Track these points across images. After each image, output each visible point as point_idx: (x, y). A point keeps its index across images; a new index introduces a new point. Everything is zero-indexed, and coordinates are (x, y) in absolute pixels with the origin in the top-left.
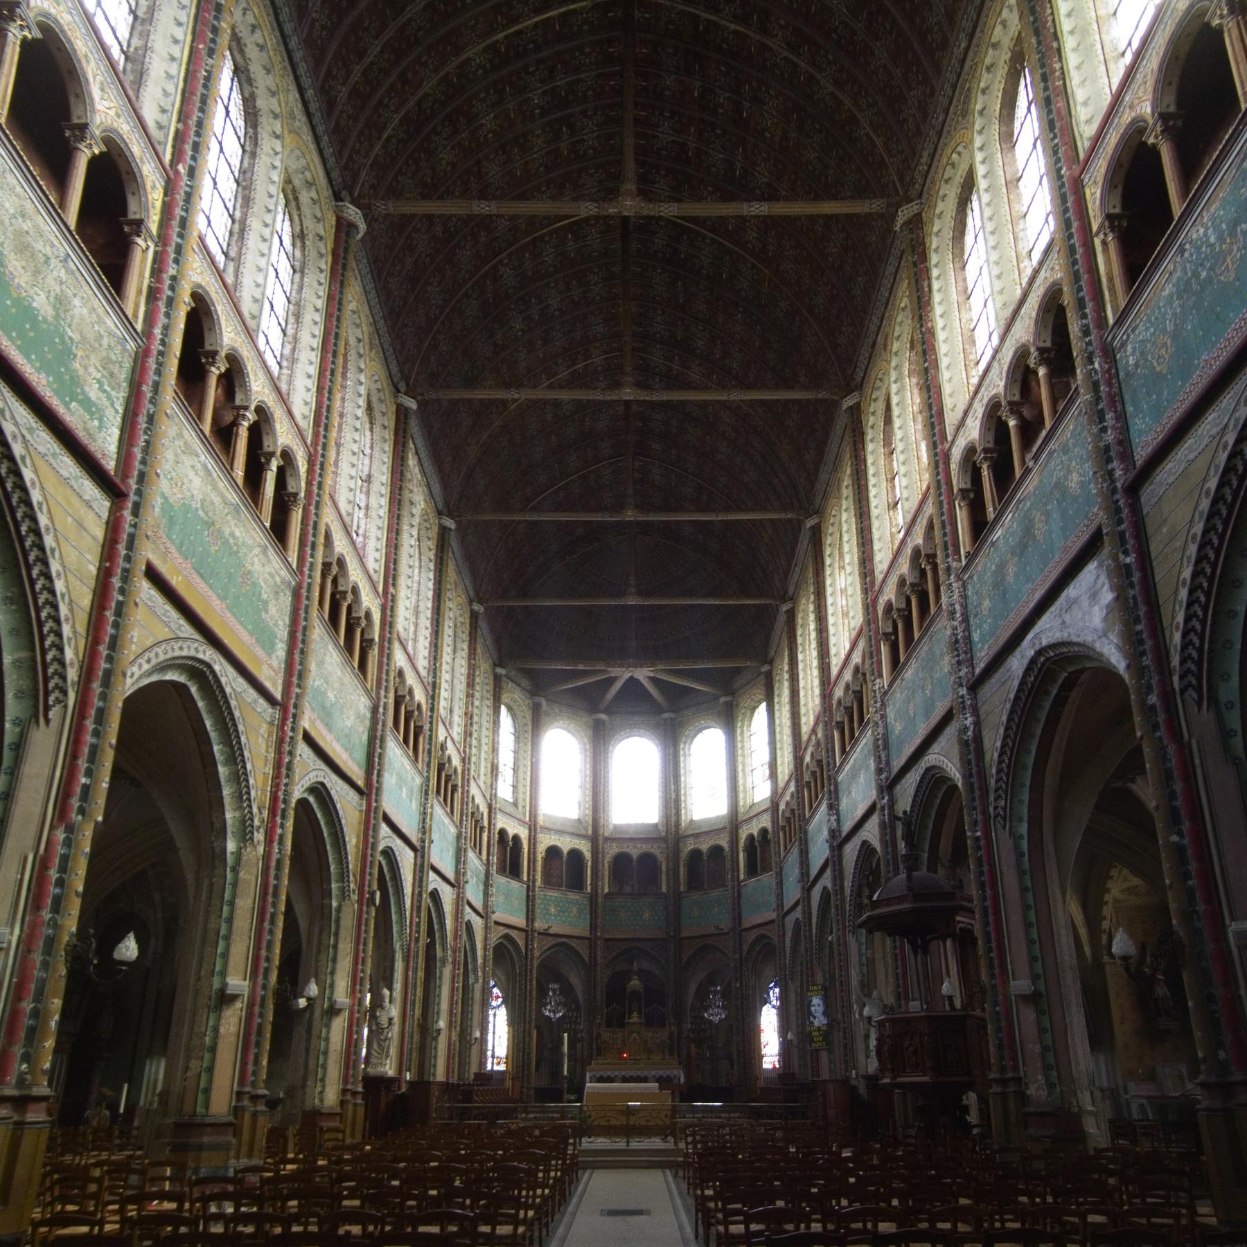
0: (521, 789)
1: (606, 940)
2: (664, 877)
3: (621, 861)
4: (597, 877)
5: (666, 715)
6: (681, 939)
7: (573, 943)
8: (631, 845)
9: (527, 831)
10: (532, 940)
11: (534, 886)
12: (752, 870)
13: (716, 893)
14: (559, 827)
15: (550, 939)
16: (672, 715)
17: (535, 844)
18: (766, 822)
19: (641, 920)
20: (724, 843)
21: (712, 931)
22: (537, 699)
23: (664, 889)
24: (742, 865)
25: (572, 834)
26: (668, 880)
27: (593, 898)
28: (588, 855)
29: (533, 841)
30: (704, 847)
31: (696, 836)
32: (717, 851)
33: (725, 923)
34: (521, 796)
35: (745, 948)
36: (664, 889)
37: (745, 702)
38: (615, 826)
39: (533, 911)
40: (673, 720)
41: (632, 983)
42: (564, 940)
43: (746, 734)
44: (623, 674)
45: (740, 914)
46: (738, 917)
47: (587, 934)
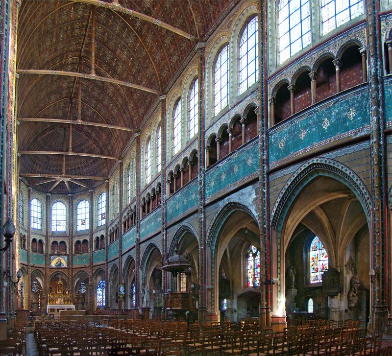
2: (68, 249)
3: (55, 243)
5: (70, 195)
12: (97, 247)
13: (84, 254)
18: (103, 233)
20: (88, 238)
24: (93, 246)
30: (81, 240)
32: (85, 241)
34: (25, 222)
40: (72, 197)
44: (59, 179)
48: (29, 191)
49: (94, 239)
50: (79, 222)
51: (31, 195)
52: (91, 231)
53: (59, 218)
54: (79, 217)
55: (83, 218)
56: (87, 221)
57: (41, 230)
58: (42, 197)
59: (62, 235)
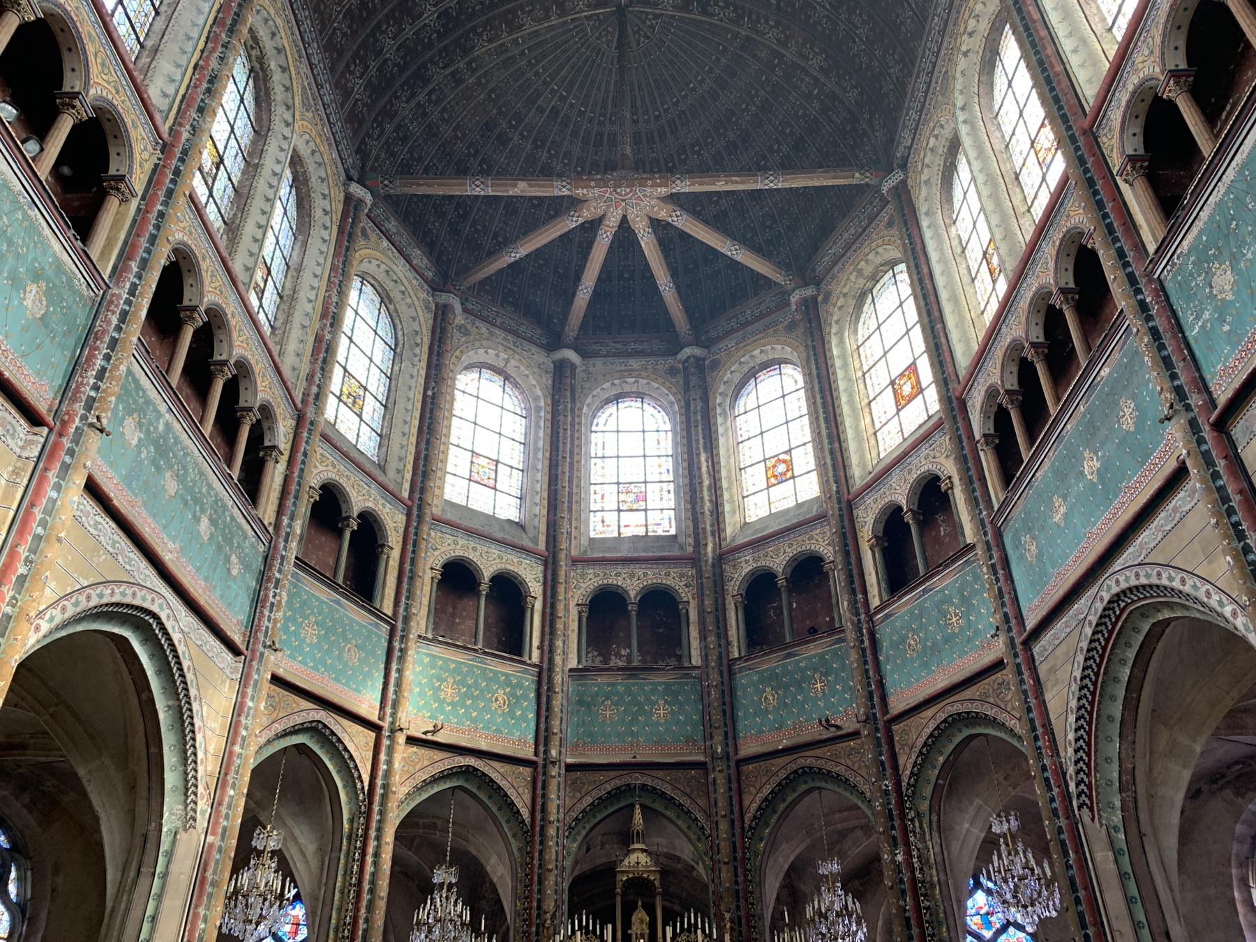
0: (396, 438)
1: (570, 768)
2: (694, 633)
4: (553, 632)
6: (739, 763)
7: (494, 771)
8: (624, 571)
9: (401, 518)
10: (391, 750)
13: (813, 651)
15: (439, 755)
16: (697, 351)
19: (647, 722)
20: (823, 544)
21: (814, 732)
22: (444, 298)
23: (696, 660)
26: (703, 637)
27: (544, 675)
28: (535, 588)
29: (412, 541)
30: (778, 561)
31: (758, 544)
32: (808, 569)
33: (848, 714)
35: (907, 762)
36: (696, 660)
37: (846, 282)
39: (399, 684)
40: (699, 361)
41: (633, 858)
42: (471, 761)
43: (850, 344)
45: (881, 684)
46: (877, 691)
47: (528, 753)
48: (441, 316)
49: (866, 533)
50: (754, 478)
51: (456, 337)
52: (842, 499)
53: (631, 471)
54: (750, 453)
55: (776, 444)
56: (805, 460)
57: (520, 526)
58: (532, 365)
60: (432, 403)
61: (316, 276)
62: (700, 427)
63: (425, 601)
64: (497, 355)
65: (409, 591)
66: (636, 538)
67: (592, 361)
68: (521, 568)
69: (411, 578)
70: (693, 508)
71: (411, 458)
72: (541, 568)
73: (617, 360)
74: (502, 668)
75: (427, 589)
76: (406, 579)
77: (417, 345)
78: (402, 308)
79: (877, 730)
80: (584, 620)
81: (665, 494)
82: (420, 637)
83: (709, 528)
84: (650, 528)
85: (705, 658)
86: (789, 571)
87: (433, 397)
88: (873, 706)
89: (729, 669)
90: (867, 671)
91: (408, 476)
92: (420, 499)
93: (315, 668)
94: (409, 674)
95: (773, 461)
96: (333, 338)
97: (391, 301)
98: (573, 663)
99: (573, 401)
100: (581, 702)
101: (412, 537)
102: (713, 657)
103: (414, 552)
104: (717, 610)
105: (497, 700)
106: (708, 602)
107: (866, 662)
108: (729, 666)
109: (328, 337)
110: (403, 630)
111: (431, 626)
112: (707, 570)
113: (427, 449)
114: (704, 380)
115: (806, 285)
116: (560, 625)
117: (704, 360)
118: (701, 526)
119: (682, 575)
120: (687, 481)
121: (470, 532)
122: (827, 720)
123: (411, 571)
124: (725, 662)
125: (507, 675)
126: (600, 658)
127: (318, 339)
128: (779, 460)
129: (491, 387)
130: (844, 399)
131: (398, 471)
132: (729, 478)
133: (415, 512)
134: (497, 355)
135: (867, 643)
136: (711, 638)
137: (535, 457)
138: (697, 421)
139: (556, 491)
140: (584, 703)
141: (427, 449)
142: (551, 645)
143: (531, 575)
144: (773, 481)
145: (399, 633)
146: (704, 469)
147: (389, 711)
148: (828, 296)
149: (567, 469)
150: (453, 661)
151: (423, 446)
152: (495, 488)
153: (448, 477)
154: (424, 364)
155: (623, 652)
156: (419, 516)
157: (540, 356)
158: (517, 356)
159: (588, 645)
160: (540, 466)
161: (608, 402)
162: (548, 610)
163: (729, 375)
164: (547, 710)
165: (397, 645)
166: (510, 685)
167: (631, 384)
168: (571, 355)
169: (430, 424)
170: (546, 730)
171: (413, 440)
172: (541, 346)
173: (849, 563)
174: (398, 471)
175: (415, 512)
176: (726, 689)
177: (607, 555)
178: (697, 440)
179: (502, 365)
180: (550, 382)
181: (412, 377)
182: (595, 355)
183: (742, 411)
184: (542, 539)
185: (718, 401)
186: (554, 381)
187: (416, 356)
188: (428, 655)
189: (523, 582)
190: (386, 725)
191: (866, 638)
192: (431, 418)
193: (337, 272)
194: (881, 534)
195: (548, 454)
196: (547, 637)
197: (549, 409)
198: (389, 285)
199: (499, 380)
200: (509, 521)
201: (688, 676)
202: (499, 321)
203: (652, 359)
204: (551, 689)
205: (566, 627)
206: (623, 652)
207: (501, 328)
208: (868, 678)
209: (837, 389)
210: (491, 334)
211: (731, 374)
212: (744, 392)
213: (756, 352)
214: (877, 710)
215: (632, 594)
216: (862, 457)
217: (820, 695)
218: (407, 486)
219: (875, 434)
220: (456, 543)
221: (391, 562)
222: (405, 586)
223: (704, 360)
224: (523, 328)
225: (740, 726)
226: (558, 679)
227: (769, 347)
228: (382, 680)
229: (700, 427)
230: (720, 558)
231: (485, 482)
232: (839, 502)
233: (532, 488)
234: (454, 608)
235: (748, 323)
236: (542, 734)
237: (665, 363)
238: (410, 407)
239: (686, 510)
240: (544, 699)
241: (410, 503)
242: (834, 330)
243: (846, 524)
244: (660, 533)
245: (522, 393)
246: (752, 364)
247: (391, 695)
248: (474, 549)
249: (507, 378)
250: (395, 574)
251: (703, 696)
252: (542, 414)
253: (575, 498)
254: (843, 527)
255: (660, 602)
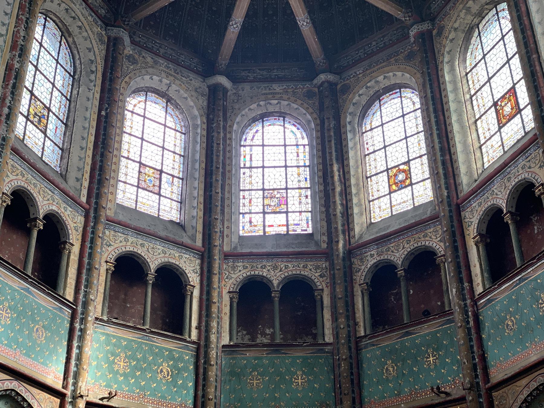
2: (327, 315)
8: (269, 264)
9: (80, 219)
11: (85, 312)
13: (426, 330)
14: (142, 225)
16: (331, 77)
17: (92, 241)
20: (435, 240)
22: (115, 32)
23: (329, 338)
25: (166, 240)
26: (335, 318)
27: (201, 350)
28: (194, 278)
29: (89, 238)
30: (398, 254)
31: (383, 240)
32: (423, 262)
36: (329, 338)
38: (241, 238)
39: (79, 358)
40: (332, 85)
43: (459, 71)
45: (483, 358)
46: (480, 363)
48: (113, 47)
49: (472, 231)
53: (275, 179)
54: (376, 163)
55: (397, 156)
56: (421, 170)
57: (181, 226)
58: (189, 90)
59: (292, 247)
60: (106, 122)
61: (6, 14)
62: (333, 142)
63: (101, 289)
64: (161, 81)
65: (87, 280)
66: (278, 236)
67: (241, 86)
68: (182, 261)
69: (89, 270)
70: (327, 211)
71: (88, 168)
72: (198, 261)
73: (263, 85)
74: (166, 345)
75: (103, 278)
76: (85, 271)
77: (92, 72)
78: (79, 40)
79: (480, 396)
80: (235, 305)
81: (304, 200)
82: (97, 319)
83: (340, 228)
84: (291, 228)
85: (336, 336)
86: (407, 263)
87: (107, 117)
88: (477, 376)
89: (356, 345)
90: (472, 347)
91: (86, 184)
92: (96, 203)
93: (9, 345)
94: (89, 350)
95: (395, 170)
96: (21, 66)
97: (70, 35)
98: (226, 340)
99: (225, 120)
100: (232, 373)
101: (90, 235)
102: (343, 334)
103: (91, 248)
104: (346, 296)
105: (162, 371)
106: (339, 289)
107: (471, 340)
108: (357, 343)
109: (17, 65)
110: (83, 314)
111: (106, 310)
112: (339, 263)
113: (101, 161)
114: (336, 102)
115: (423, 21)
116: (214, 309)
117: (336, 84)
118: (334, 226)
119: (317, 267)
120: (322, 188)
121: (139, 231)
122: (438, 388)
123: (89, 264)
124: (353, 339)
125: (171, 351)
126: (248, 337)
127: (9, 68)
128: (400, 171)
129: (156, 109)
130: (454, 118)
131: (78, 180)
132: (357, 185)
133: (92, 215)
134: (161, 81)
135: (472, 323)
136: (342, 320)
137: (193, 168)
138: (330, 136)
139: (211, 196)
140: (235, 374)
141: (101, 161)
142: (208, 326)
143: (190, 267)
144: (394, 187)
145: (79, 316)
146: (336, 178)
147: (71, 381)
148: (441, 30)
149: (220, 178)
150: (125, 339)
151: (98, 158)
152: (159, 194)
153: (121, 185)
154: (98, 89)
155: (268, 331)
156: (95, 217)
157: (197, 82)
158: (177, 82)
159: (238, 326)
160: (197, 175)
161: (254, 120)
162: (204, 297)
163: (357, 98)
164: (205, 379)
165: (77, 326)
166: (173, 359)
167: (274, 105)
168: (223, 80)
169: (104, 140)
170: (203, 396)
171: (90, 153)
172: (197, 73)
173: (457, 257)
174: (78, 180)
175: (92, 215)
176: (354, 362)
177: (255, 251)
178: (331, 153)
179: (164, 89)
180: (205, 103)
181: (88, 99)
182: (244, 80)
183: (368, 128)
184: (199, 237)
185: (348, 120)
186: (209, 103)
187: (91, 81)
188: (103, 334)
189: (183, 273)
190: (68, 392)
191: (471, 320)
192: (104, 135)
193: (24, 10)
194: (484, 232)
195: (203, 165)
196: (204, 319)
197: (205, 126)
198: (68, 21)
199: (162, 102)
200: (171, 222)
201: (322, 351)
202: (162, 51)
203: (292, 85)
204: (207, 361)
205: (219, 311)
206: (268, 331)
207: (164, 57)
208: (473, 352)
209: (448, 110)
210: (156, 62)
211: (359, 97)
212: (370, 112)
213: (381, 78)
214: (480, 380)
215: (275, 283)
216: (469, 167)
217: (432, 367)
218: (85, 192)
219: (480, 147)
220: (126, 240)
221: (72, 257)
222: (84, 277)
223: (336, 84)
224: (182, 58)
225: (365, 393)
226: (213, 353)
227: (391, 74)
228: (65, 355)
229: (333, 142)
230: (350, 253)
231: (151, 189)
232: (450, 205)
233: (191, 193)
234: (126, 295)
235: (373, 54)
236: (200, 400)
237: (303, 87)
238: (87, 125)
239: (321, 212)
240: (201, 371)
241: (87, 206)
242: (446, 59)
243: (455, 223)
244: (299, 231)
245: (182, 113)
246: (377, 89)
247: (73, 368)
248: (142, 245)
249: (169, 100)
250: (76, 266)
251: (334, 368)
252: (199, 131)
253: (227, 202)
254: (452, 226)
255: (298, 290)
